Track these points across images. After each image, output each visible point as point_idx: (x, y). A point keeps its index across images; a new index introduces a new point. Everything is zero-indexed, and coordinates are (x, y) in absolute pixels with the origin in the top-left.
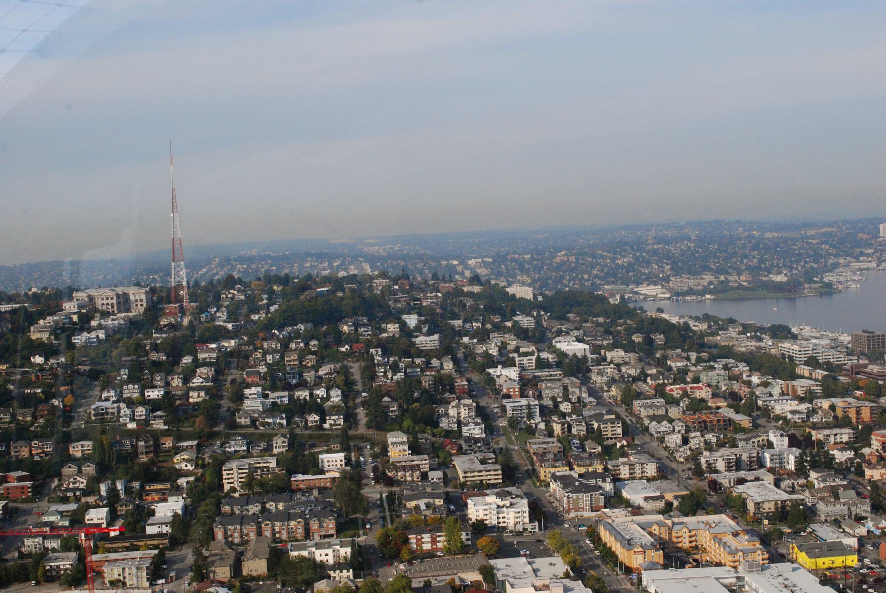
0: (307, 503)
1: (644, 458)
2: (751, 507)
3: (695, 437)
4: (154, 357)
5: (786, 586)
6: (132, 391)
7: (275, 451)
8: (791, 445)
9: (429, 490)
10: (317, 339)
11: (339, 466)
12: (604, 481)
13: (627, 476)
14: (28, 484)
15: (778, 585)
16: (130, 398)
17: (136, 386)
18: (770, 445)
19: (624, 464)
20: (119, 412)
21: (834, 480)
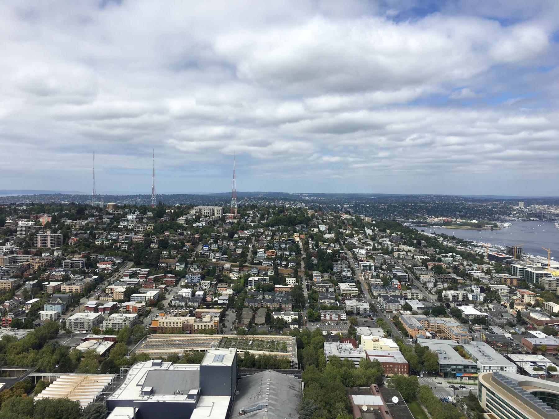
0: (280, 296)
1: (418, 291)
2: (464, 316)
3: (440, 284)
4: (223, 234)
5: (481, 352)
6: (214, 247)
7: (269, 274)
8: (481, 292)
9: (329, 296)
10: (286, 232)
11: (293, 283)
12: (401, 299)
13: (410, 298)
14: (174, 279)
15: (477, 351)
16: (214, 249)
17: (216, 245)
18: (472, 291)
19: (409, 293)
20: (209, 255)
21: (501, 308)
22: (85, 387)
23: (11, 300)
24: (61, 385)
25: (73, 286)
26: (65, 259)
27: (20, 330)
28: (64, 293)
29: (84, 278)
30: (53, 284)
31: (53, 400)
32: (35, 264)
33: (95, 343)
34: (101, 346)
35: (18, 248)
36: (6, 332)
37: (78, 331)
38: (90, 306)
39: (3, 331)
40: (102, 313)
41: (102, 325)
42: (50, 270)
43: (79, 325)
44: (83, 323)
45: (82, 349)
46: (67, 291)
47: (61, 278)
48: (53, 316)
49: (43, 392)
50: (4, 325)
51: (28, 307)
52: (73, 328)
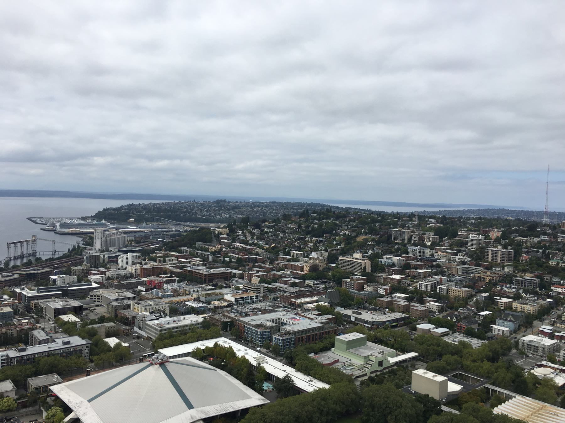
22: (544, 417)
23: (465, 309)
24: (518, 406)
25: (525, 306)
26: (516, 276)
27: (473, 339)
28: (515, 311)
29: (538, 299)
30: (504, 300)
31: (512, 419)
32: (486, 277)
33: (551, 372)
34: (558, 377)
35: (470, 259)
36: (461, 338)
37: (532, 354)
38: (545, 330)
39: (458, 336)
40: (559, 342)
41: (558, 354)
42: (502, 286)
43: (532, 348)
44: (537, 347)
45: (538, 374)
46: (519, 310)
47: (513, 296)
48: (505, 332)
49: (499, 406)
50: (458, 330)
51: (481, 318)
52: (526, 350)
